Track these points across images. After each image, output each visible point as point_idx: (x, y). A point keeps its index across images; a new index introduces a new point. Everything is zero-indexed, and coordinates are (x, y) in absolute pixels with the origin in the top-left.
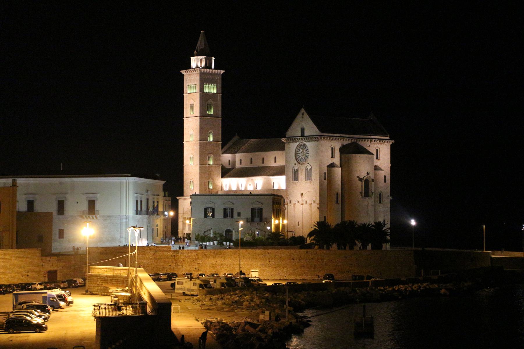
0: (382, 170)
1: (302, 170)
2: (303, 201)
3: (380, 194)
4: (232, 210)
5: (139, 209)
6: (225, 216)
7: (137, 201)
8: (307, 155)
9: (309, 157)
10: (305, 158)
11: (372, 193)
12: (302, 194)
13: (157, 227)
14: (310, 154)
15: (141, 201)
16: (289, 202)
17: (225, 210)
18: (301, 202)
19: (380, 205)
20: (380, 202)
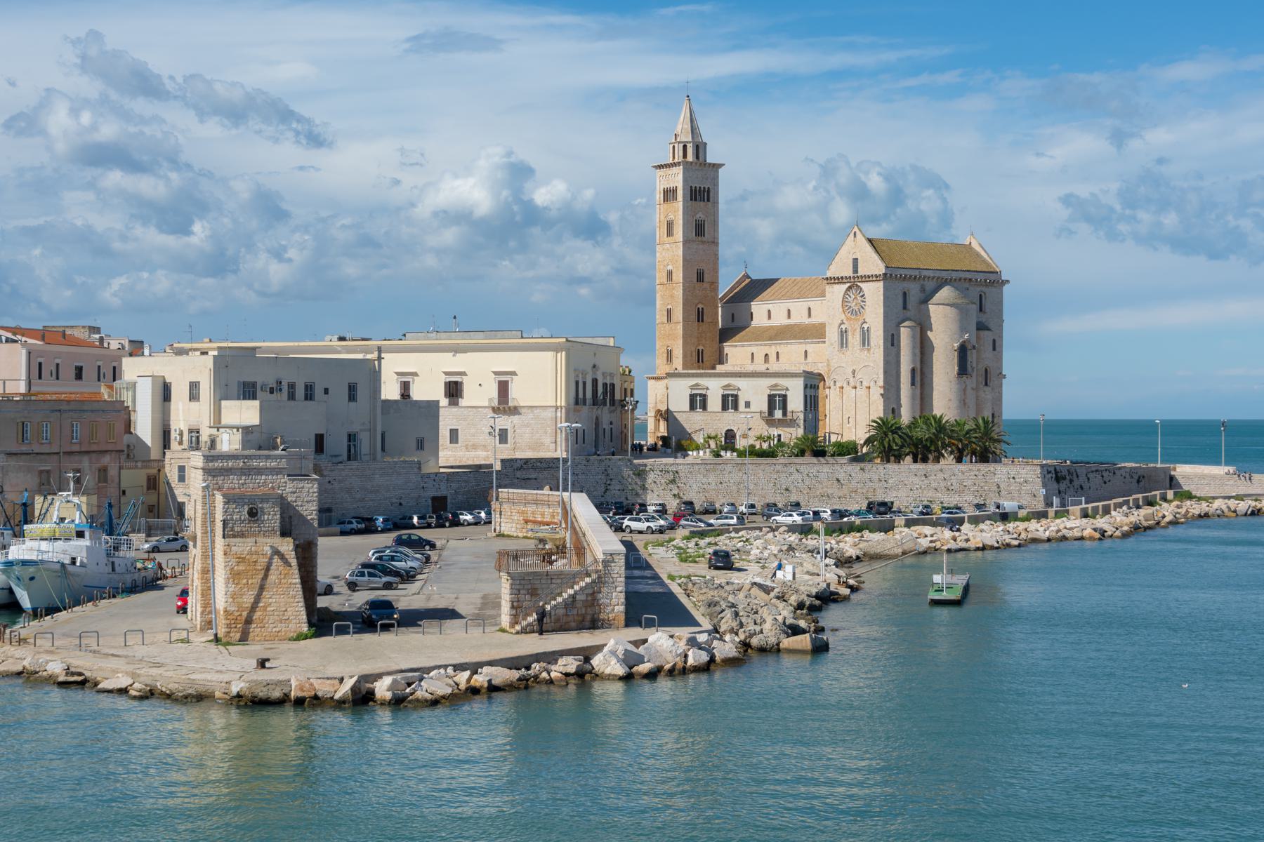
0: (988, 329)
1: (855, 330)
2: (855, 382)
3: (986, 370)
4: (736, 397)
5: (581, 395)
6: (725, 407)
7: (577, 383)
8: (862, 304)
11: (973, 369)
12: (854, 372)
14: (867, 303)
15: (584, 384)
16: (832, 383)
18: (852, 384)
19: (986, 389)
20: (986, 384)
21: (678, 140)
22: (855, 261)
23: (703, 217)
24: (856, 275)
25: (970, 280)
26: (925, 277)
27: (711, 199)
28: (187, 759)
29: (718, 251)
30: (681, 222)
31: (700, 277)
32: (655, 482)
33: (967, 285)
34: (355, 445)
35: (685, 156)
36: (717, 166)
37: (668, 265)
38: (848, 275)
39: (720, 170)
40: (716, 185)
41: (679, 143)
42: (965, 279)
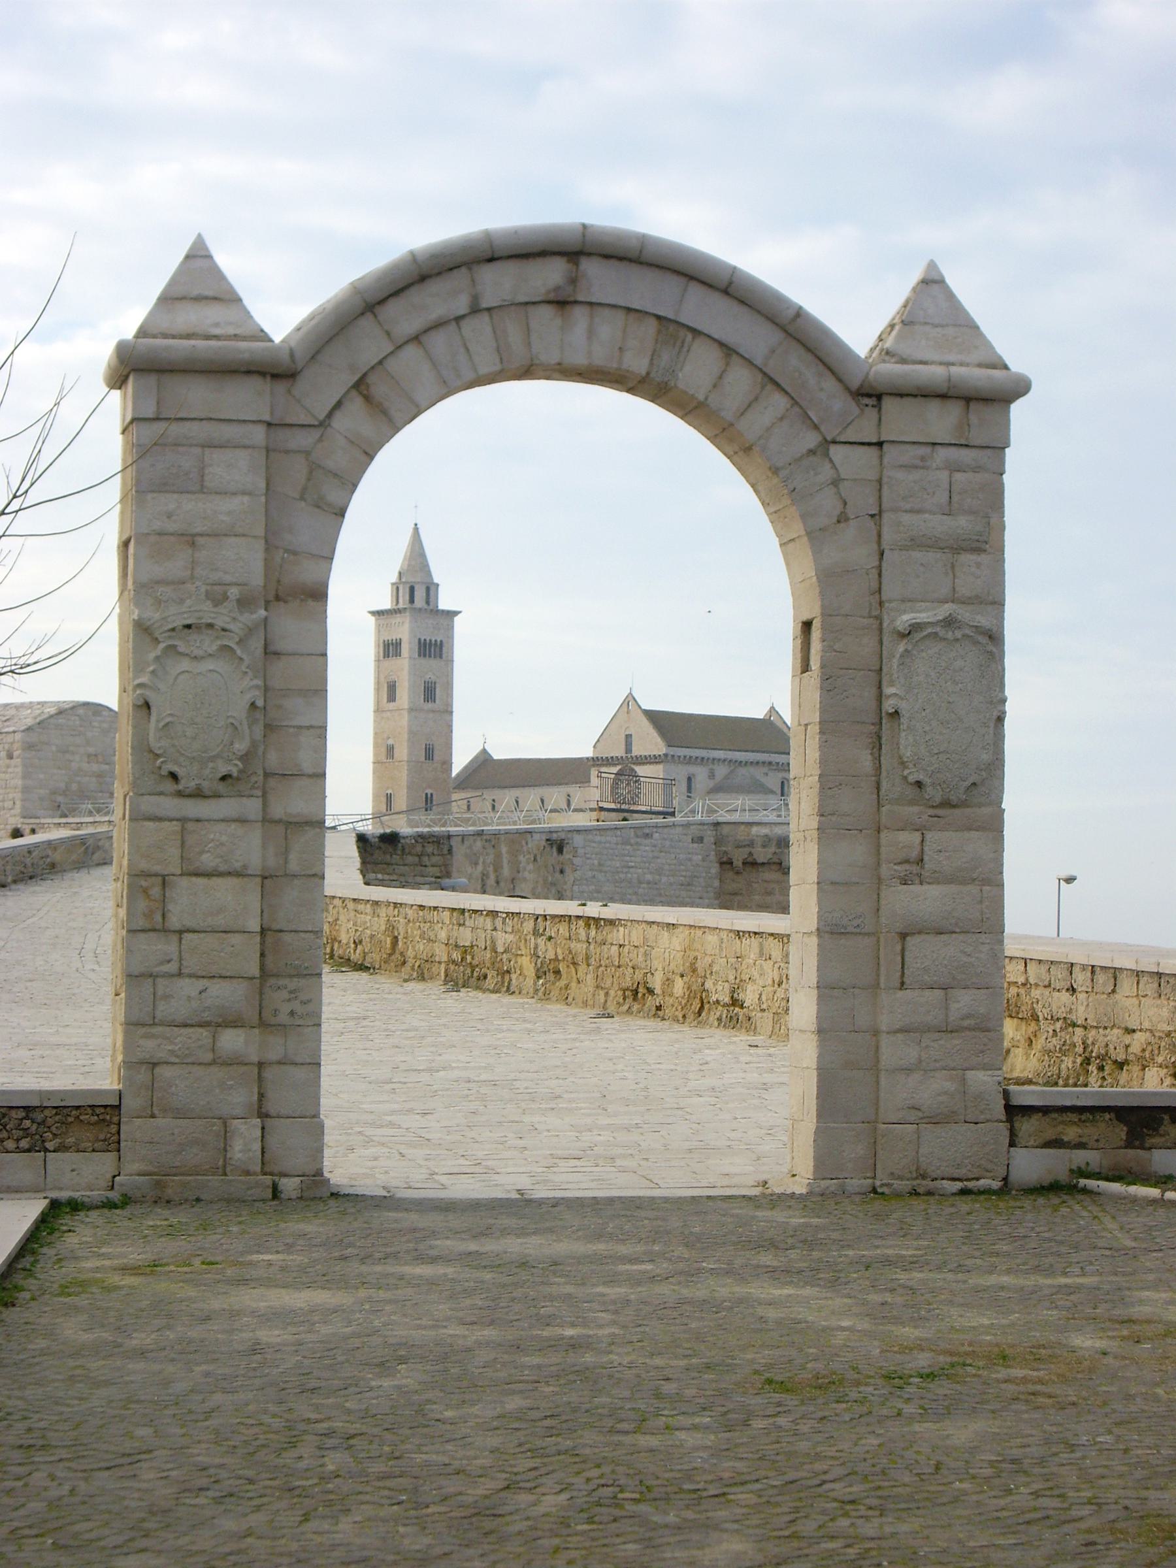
21: (403, 580)
22: (628, 737)
23: (433, 678)
24: (629, 756)
25: (770, 763)
26: (714, 759)
27: (444, 656)
29: (452, 721)
30: (406, 684)
31: (429, 753)
33: (765, 770)
35: (412, 601)
36: (452, 614)
37: (389, 738)
38: (619, 755)
39: (456, 619)
40: (451, 637)
41: (404, 583)
42: (764, 763)
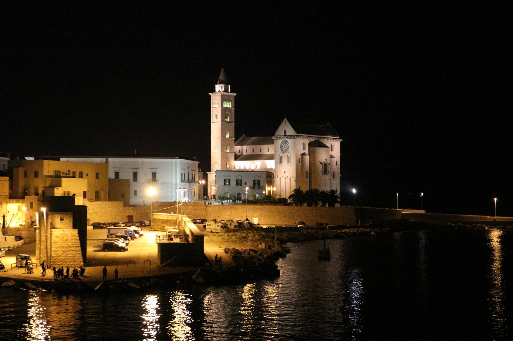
0: (335, 158)
1: (285, 157)
3: (334, 173)
4: (241, 180)
5: (183, 179)
6: (237, 184)
7: (182, 174)
8: (288, 147)
9: (289, 148)
10: (287, 149)
12: (285, 172)
13: (195, 191)
14: (290, 147)
15: (185, 174)
16: (277, 176)
17: (237, 181)
18: (284, 177)
19: (334, 179)
28: (49, 247)
32: (211, 212)
34: (98, 196)
